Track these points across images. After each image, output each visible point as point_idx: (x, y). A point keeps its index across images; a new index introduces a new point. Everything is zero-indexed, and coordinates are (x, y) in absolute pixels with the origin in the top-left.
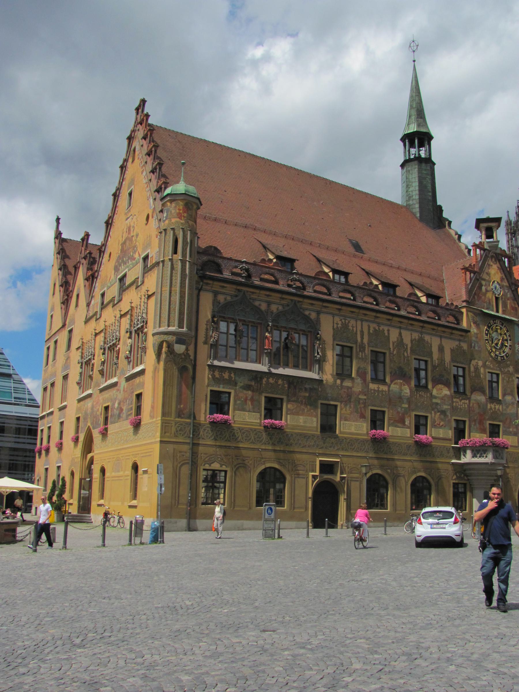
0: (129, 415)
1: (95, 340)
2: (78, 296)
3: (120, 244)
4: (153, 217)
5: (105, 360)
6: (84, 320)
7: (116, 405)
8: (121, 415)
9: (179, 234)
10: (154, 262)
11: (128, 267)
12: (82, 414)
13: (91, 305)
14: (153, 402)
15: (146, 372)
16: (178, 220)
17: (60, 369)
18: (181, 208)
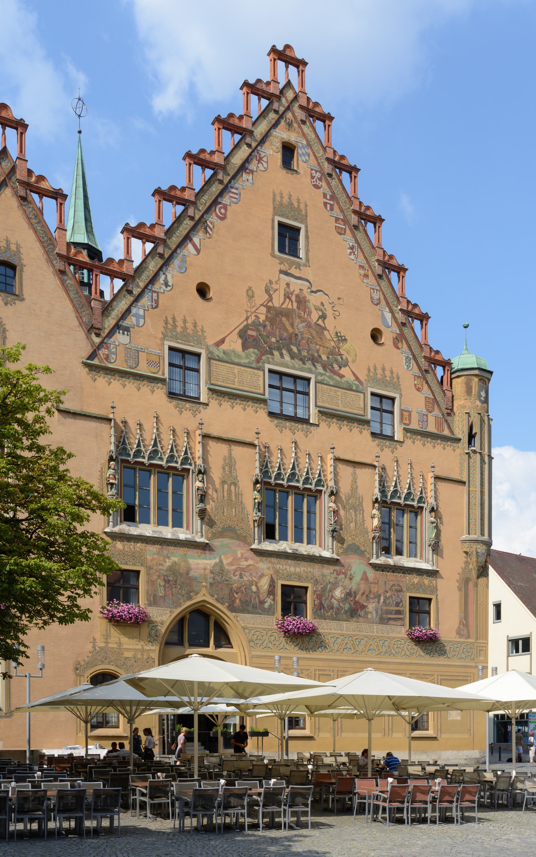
0: (390, 619)
7: (338, 593)
8: (359, 612)
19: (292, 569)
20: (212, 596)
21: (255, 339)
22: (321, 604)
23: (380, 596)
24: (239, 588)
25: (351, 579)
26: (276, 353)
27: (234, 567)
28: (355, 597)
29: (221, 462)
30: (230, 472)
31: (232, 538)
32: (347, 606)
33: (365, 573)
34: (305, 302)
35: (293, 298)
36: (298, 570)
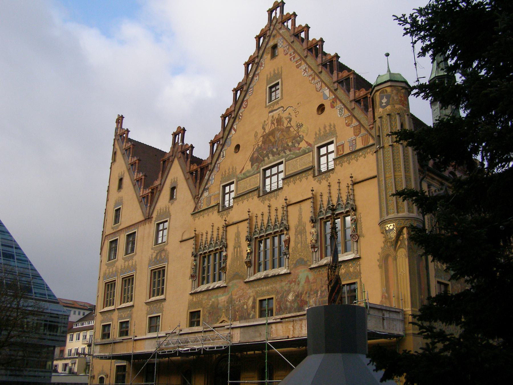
1: (226, 231)
2: (173, 189)
3: (259, 136)
4: (333, 107)
5: (251, 252)
6: (191, 211)
7: (290, 297)
9: (404, 120)
10: (347, 151)
11: (282, 157)
12: (204, 308)
13: (203, 197)
14: (388, 291)
15: (361, 261)
16: (401, 106)
17: (146, 261)
18: (402, 95)
19: (265, 288)
20: (227, 317)
21: (257, 158)
22: (280, 307)
23: (318, 291)
24: (238, 309)
25: (298, 284)
26: (266, 159)
27: (236, 297)
28: (301, 297)
29: (234, 236)
30: (238, 240)
31: (237, 279)
32: (296, 305)
33: (307, 277)
34: (281, 119)
35: (275, 122)
36: (268, 288)
